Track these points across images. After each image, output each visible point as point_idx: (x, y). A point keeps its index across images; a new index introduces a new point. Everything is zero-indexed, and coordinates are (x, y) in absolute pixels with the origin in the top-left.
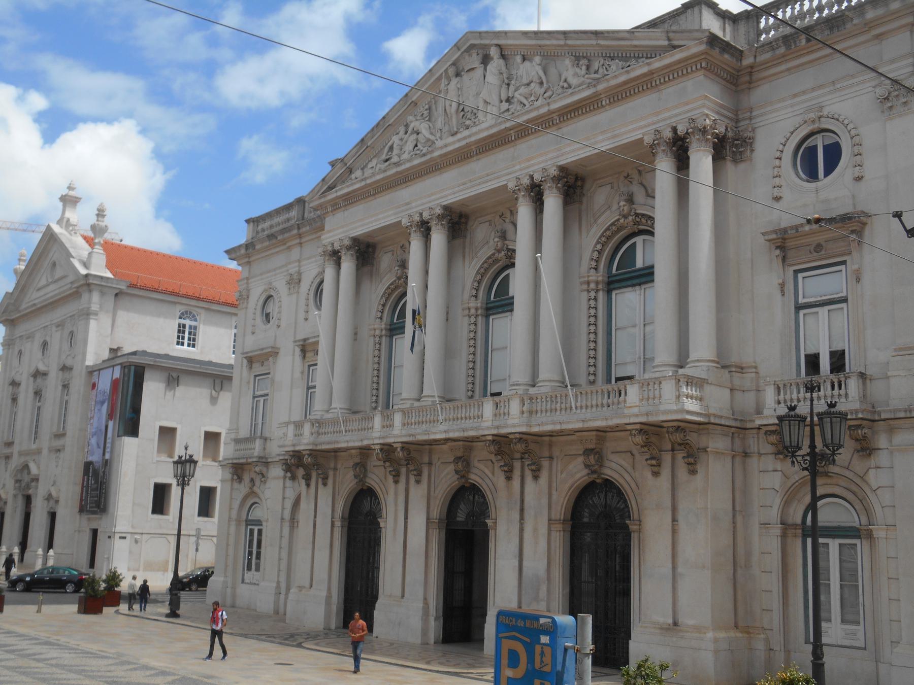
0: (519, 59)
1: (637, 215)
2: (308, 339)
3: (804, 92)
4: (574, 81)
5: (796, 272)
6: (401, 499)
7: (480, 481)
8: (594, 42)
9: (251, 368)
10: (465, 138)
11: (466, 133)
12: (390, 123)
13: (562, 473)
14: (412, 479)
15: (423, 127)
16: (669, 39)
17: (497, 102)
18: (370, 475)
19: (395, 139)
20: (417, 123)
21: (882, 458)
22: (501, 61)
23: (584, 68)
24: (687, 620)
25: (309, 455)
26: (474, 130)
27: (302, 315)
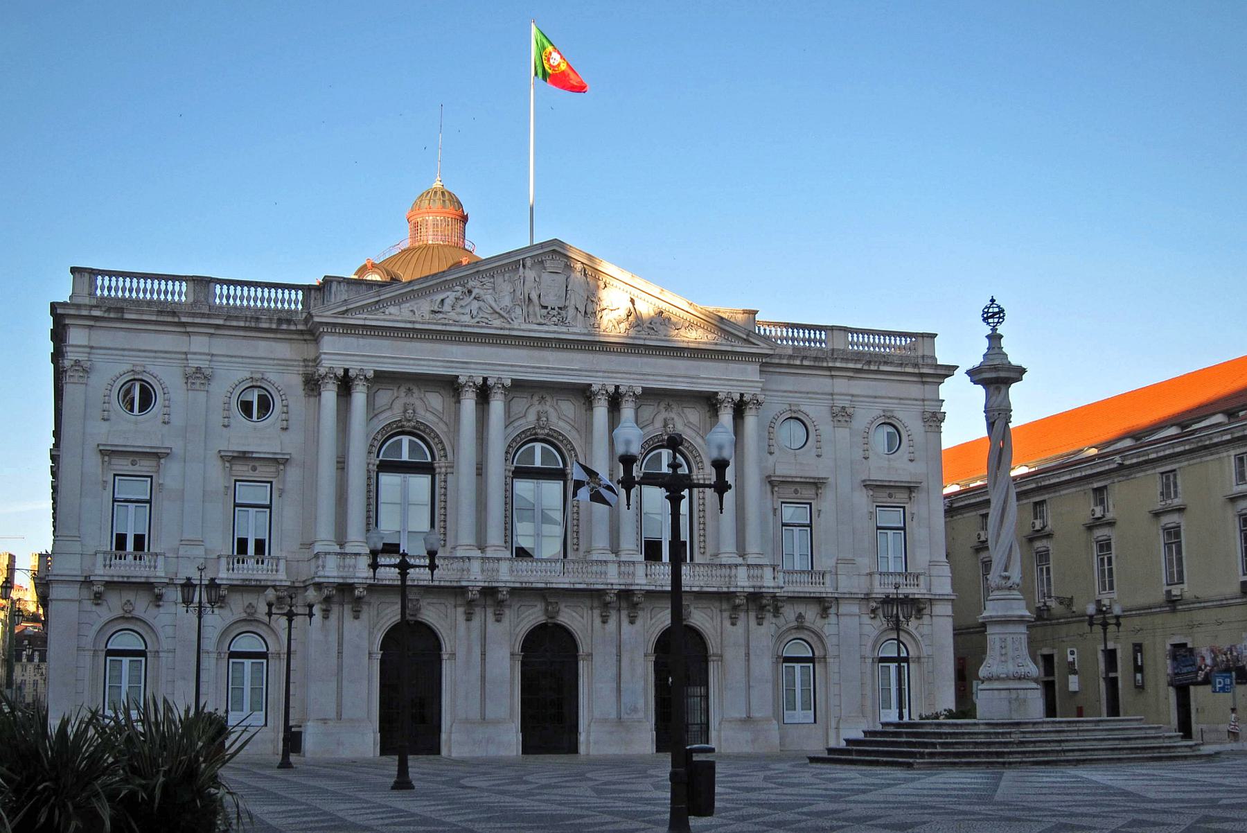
2: (252, 452)
5: (782, 503)
6: (475, 634)
10: (554, 332)
11: (556, 328)
12: (448, 278)
13: (651, 619)
15: (490, 299)
16: (748, 335)
18: (423, 611)
19: (450, 296)
20: (482, 292)
21: (833, 619)
24: (756, 714)
26: (564, 329)
27: (217, 419)
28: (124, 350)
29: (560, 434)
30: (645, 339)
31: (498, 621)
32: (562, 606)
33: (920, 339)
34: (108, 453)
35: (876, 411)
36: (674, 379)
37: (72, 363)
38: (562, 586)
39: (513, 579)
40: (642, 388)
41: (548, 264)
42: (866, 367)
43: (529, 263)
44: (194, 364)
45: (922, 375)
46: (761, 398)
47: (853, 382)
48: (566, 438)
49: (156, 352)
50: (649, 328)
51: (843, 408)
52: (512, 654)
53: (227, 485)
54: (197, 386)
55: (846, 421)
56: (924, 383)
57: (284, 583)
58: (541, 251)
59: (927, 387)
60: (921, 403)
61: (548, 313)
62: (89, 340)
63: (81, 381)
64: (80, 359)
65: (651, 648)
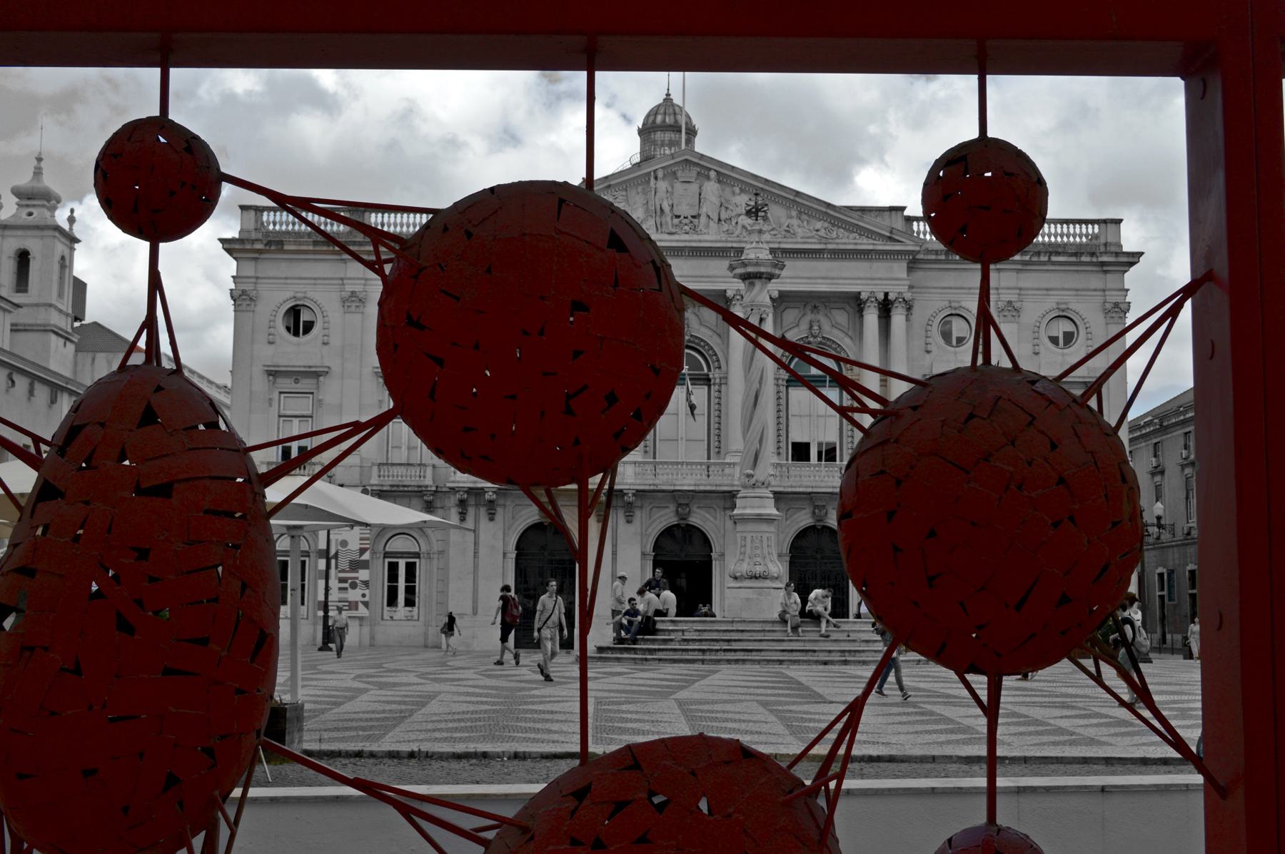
0: (737, 190)
1: (823, 338)
3: (950, 288)
4: (800, 232)
7: (702, 524)
8: (824, 210)
9: (274, 383)
11: (686, 237)
13: (786, 520)
14: (622, 520)
16: (891, 232)
17: (716, 221)
22: (718, 185)
23: (805, 223)
25: (494, 492)
26: (695, 237)
28: (286, 278)
29: (702, 340)
30: (780, 243)
31: (629, 522)
32: (694, 509)
33: (1103, 225)
34: (274, 374)
35: (1050, 303)
36: (813, 281)
37: (240, 292)
38: (686, 488)
39: (638, 482)
40: (779, 291)
41: (679, 174)
42: (1035, 259)
43: (660, 174)
44: (349, 288)
45: (1103, 264)
46: (908, 296)
47: (1022, 275)
48: (708, 344)
49: (315, 279)
50: (786, 231)
51: (1010, 303)
52: (644, 554)
53: (381, 399)
54: (353, 309)
55: (1013, 316)
56: (1106, 272)
57: (429, 489)
58: (672, 162)
59: (1109, 276)
60: (1101, 293)
61: (680, 222)
62: (256, 271)
63: (249, 308)
64: (246, 288)
65: (786, 548)
